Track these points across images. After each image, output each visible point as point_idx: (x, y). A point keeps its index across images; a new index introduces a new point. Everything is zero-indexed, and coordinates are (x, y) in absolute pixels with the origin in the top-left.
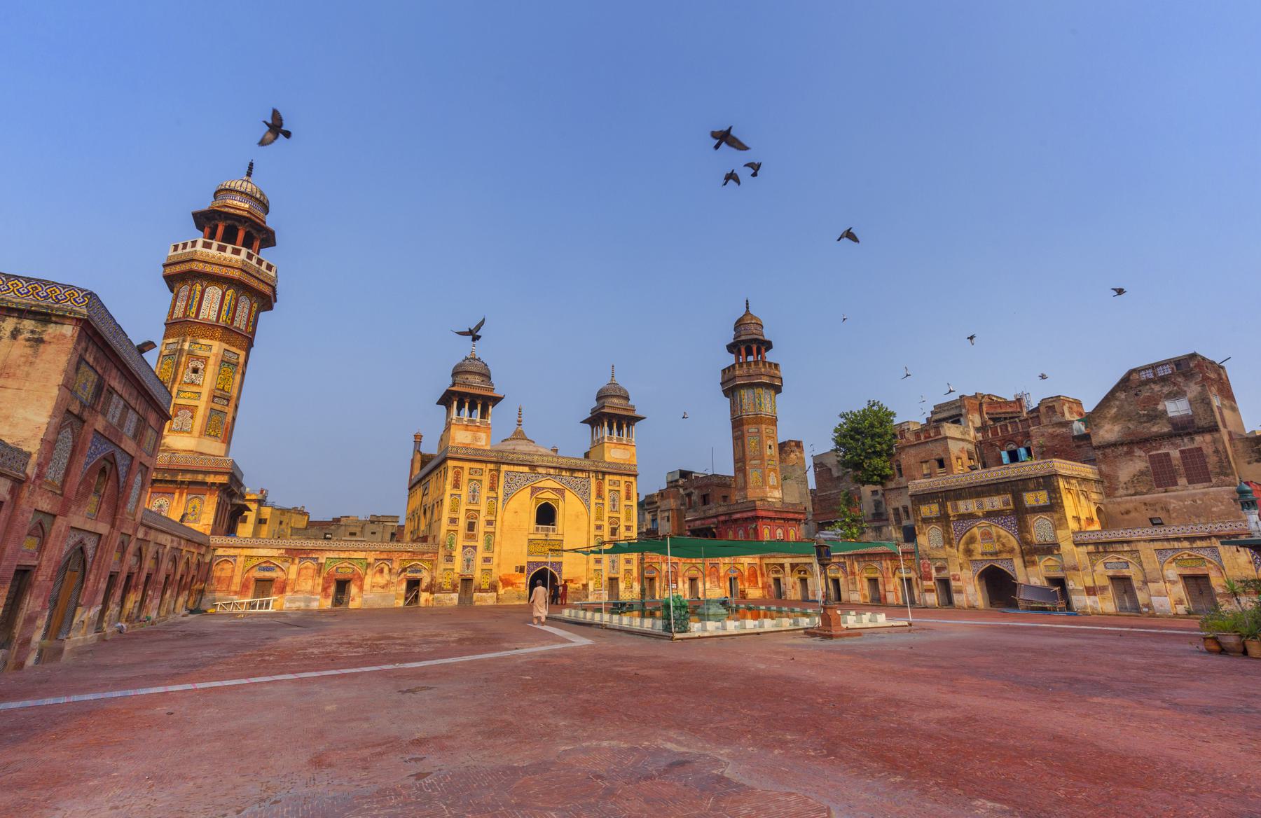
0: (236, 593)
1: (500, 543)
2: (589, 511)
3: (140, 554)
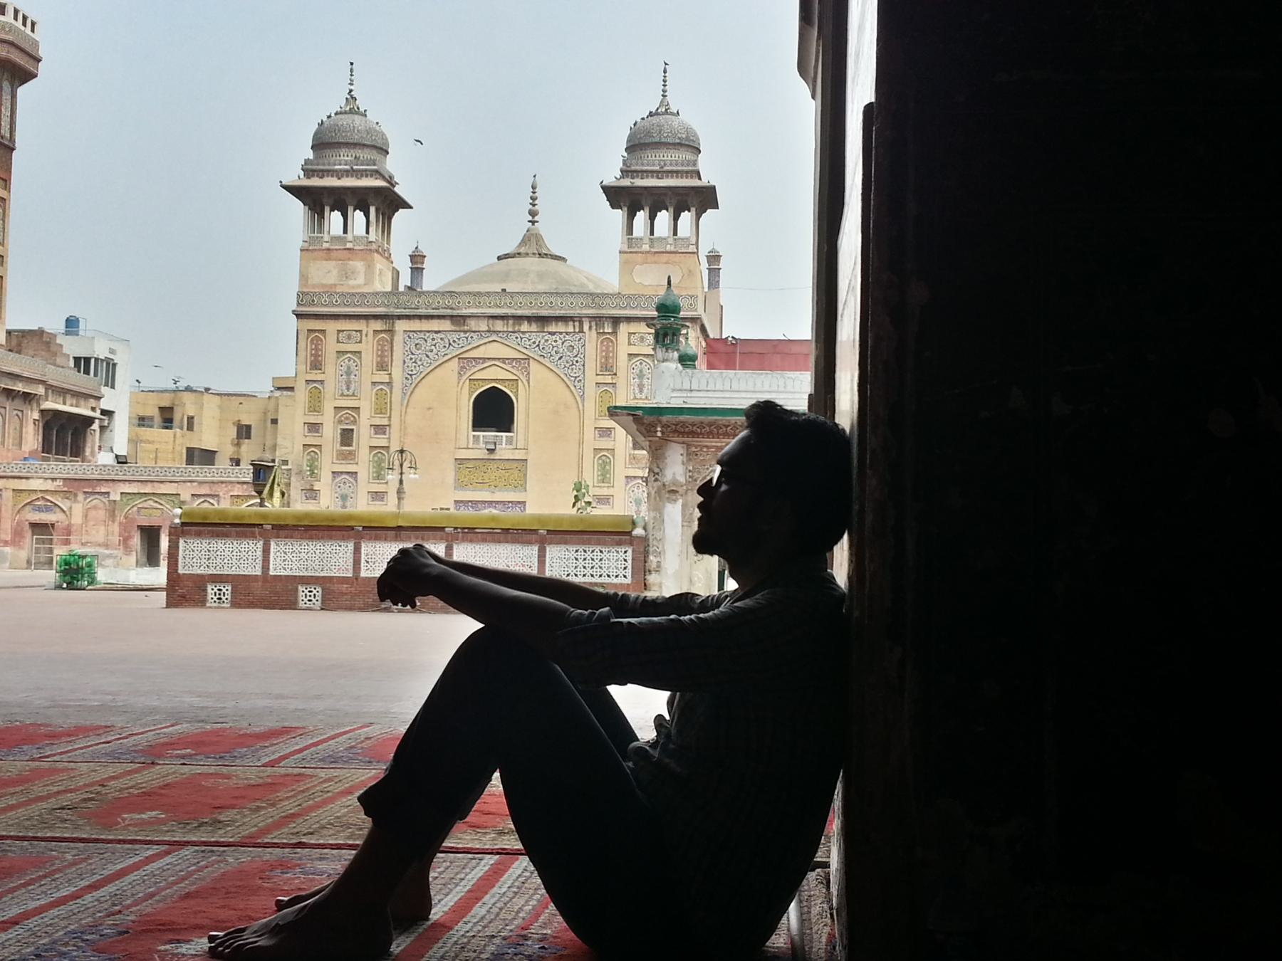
2: (583, 401)
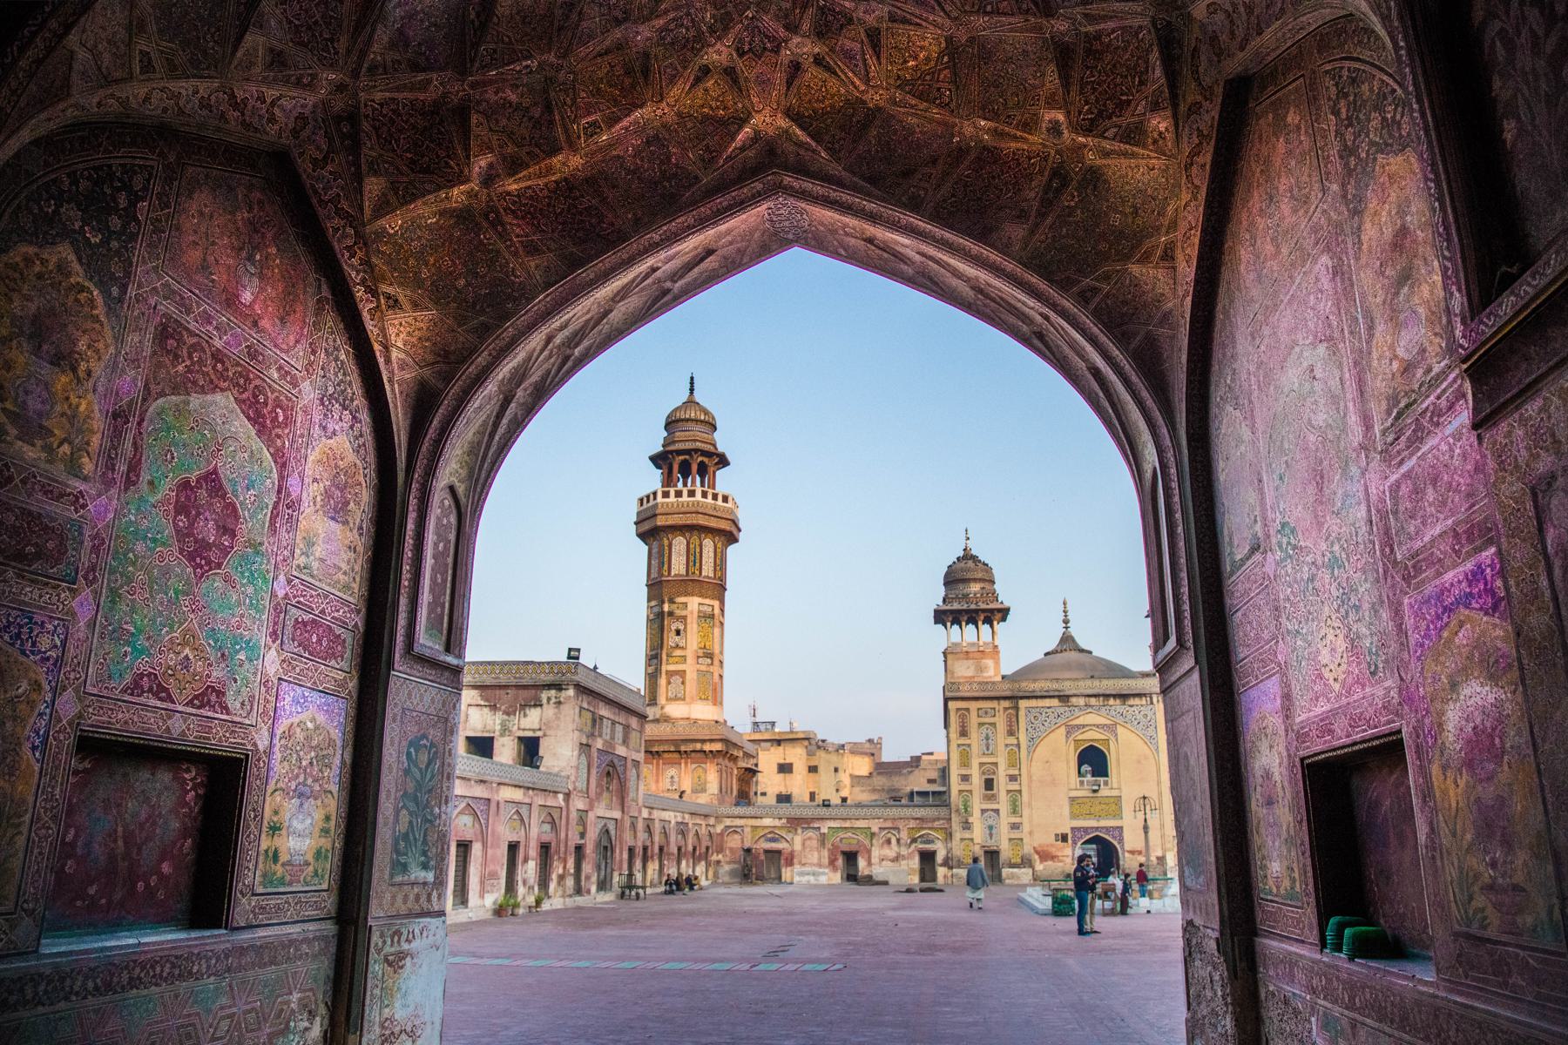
1: (1030, 804)
3: (649, 830)
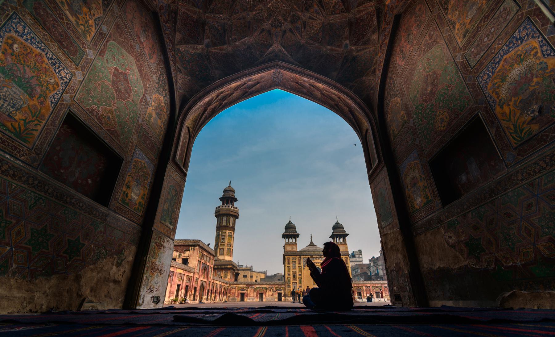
0: (236, 297)
1: (304, 281)
3: (213, 286)
